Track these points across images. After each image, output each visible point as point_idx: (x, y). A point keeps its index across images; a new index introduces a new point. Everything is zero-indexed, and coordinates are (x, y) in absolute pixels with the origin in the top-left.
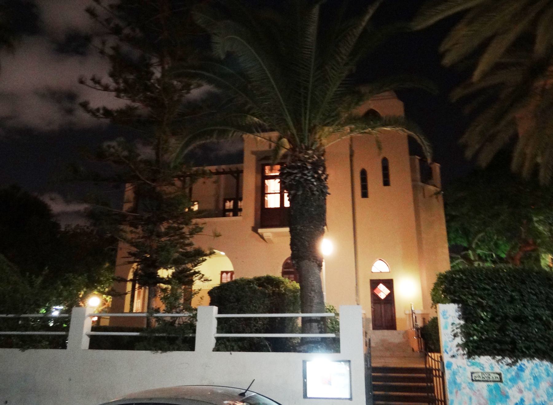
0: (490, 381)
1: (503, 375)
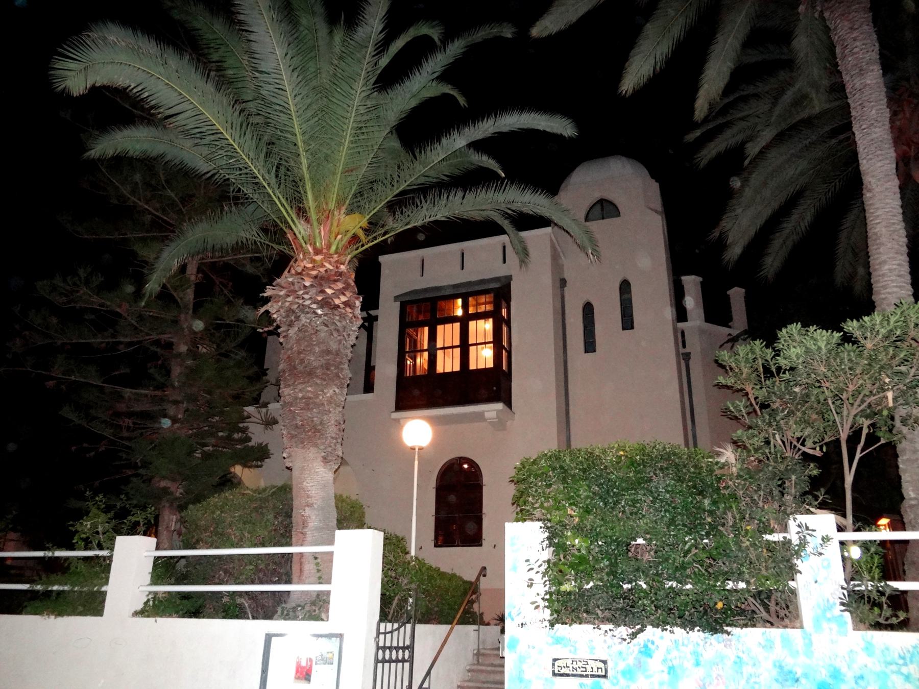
0: (587, 676)
1: (610, 665)
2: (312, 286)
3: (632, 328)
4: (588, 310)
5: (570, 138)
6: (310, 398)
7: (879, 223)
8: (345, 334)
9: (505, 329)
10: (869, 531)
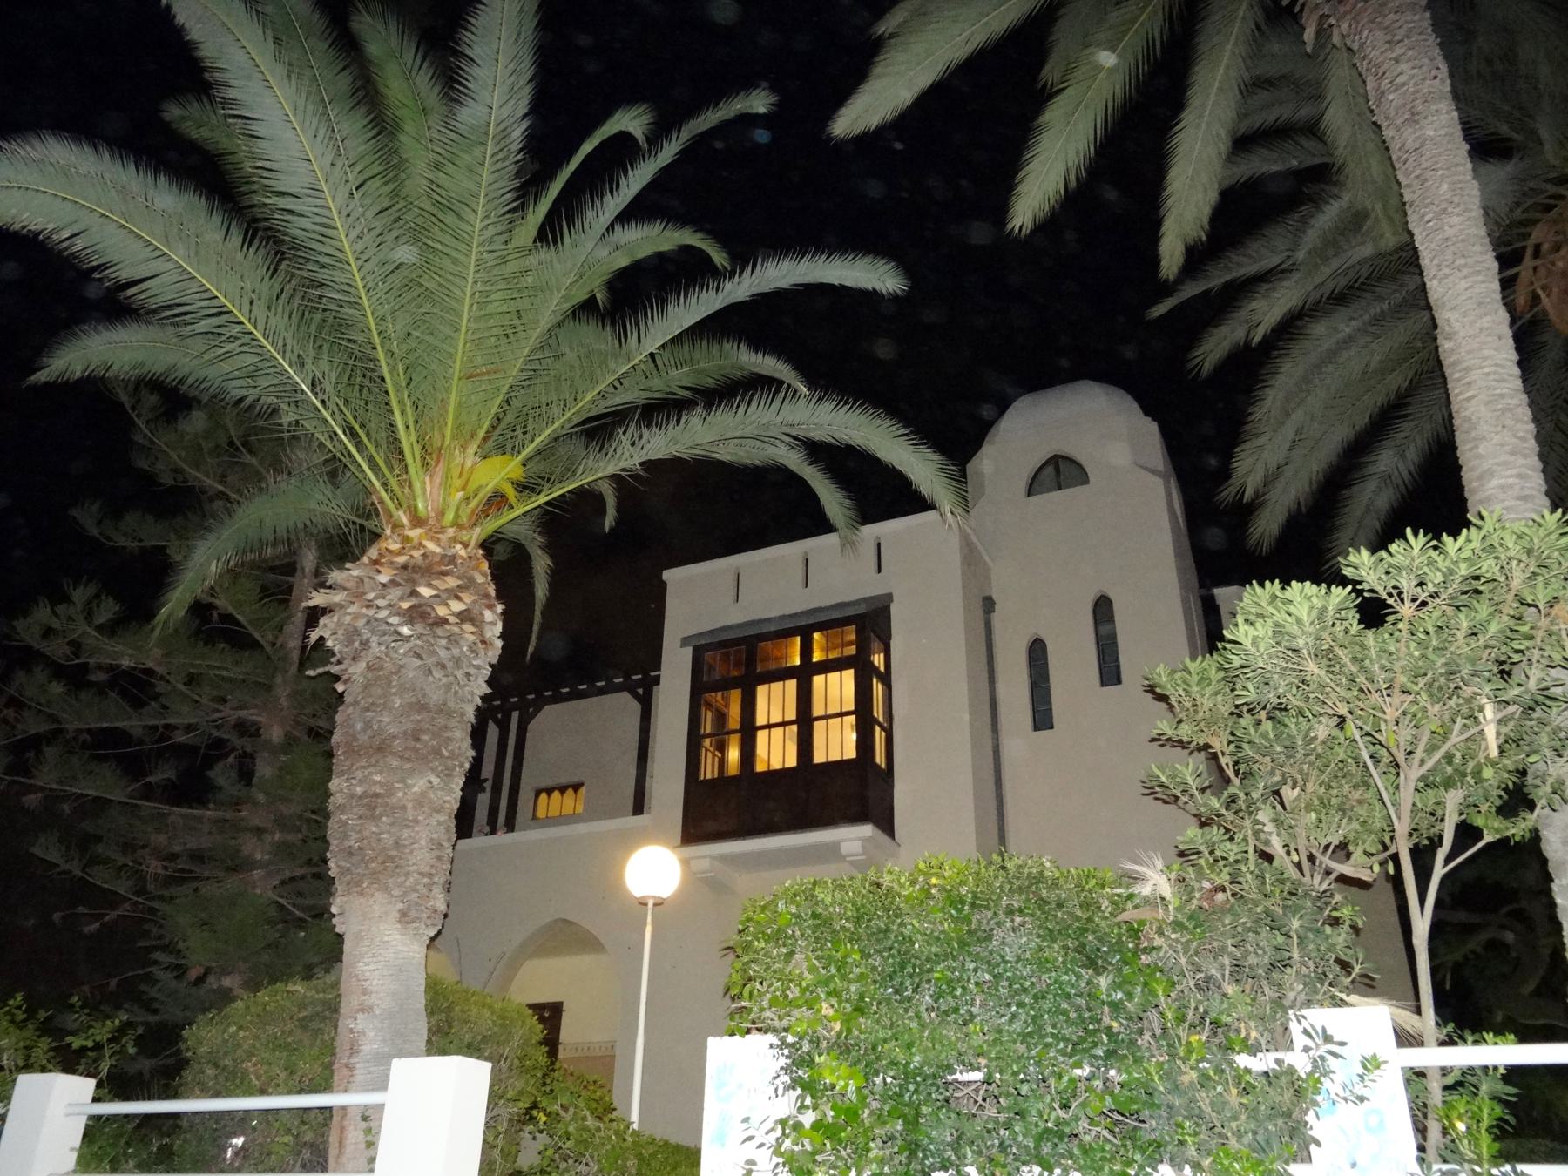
2: (393, 583)
3: (1119, 681)
4: (1037, 652)
5: (895, 298)
6: (377, 795)
7: (1473, 397)
8: (459, 674)
9: (878, 689)
10: (1476, 1042)
